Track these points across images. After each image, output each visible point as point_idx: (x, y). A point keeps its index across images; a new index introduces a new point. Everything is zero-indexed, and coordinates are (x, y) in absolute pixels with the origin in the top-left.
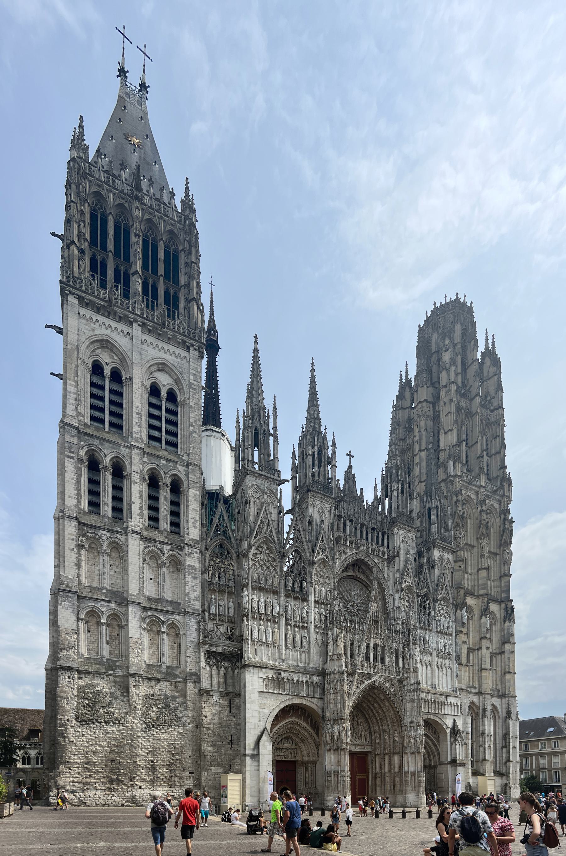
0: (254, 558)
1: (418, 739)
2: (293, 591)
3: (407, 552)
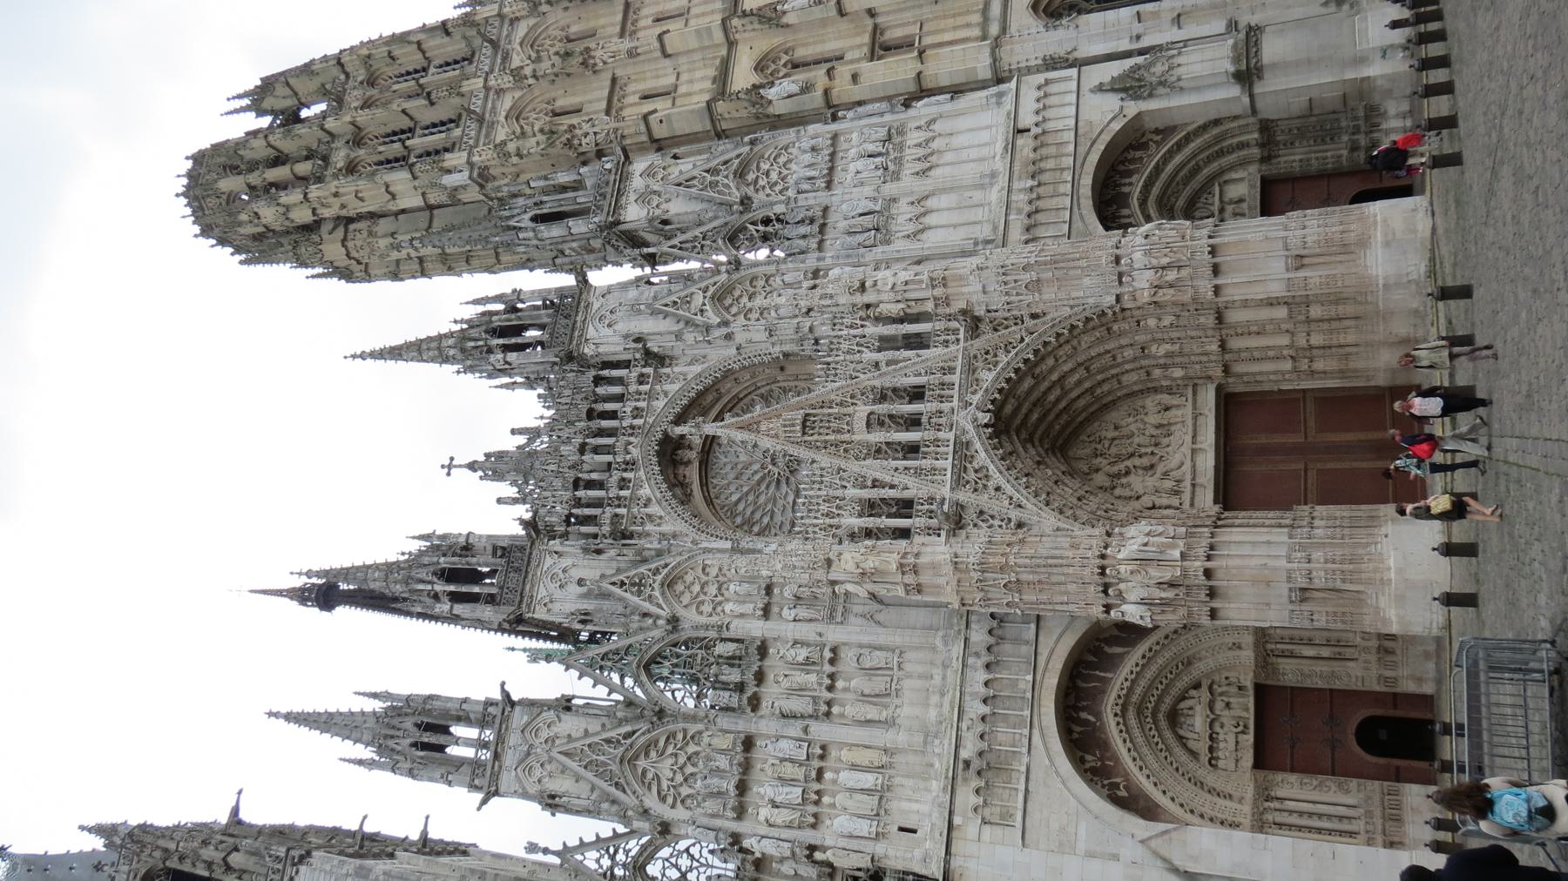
0: (670, 800)
1: (1165, 261)
2: (740, 688)
3: (635, 309)
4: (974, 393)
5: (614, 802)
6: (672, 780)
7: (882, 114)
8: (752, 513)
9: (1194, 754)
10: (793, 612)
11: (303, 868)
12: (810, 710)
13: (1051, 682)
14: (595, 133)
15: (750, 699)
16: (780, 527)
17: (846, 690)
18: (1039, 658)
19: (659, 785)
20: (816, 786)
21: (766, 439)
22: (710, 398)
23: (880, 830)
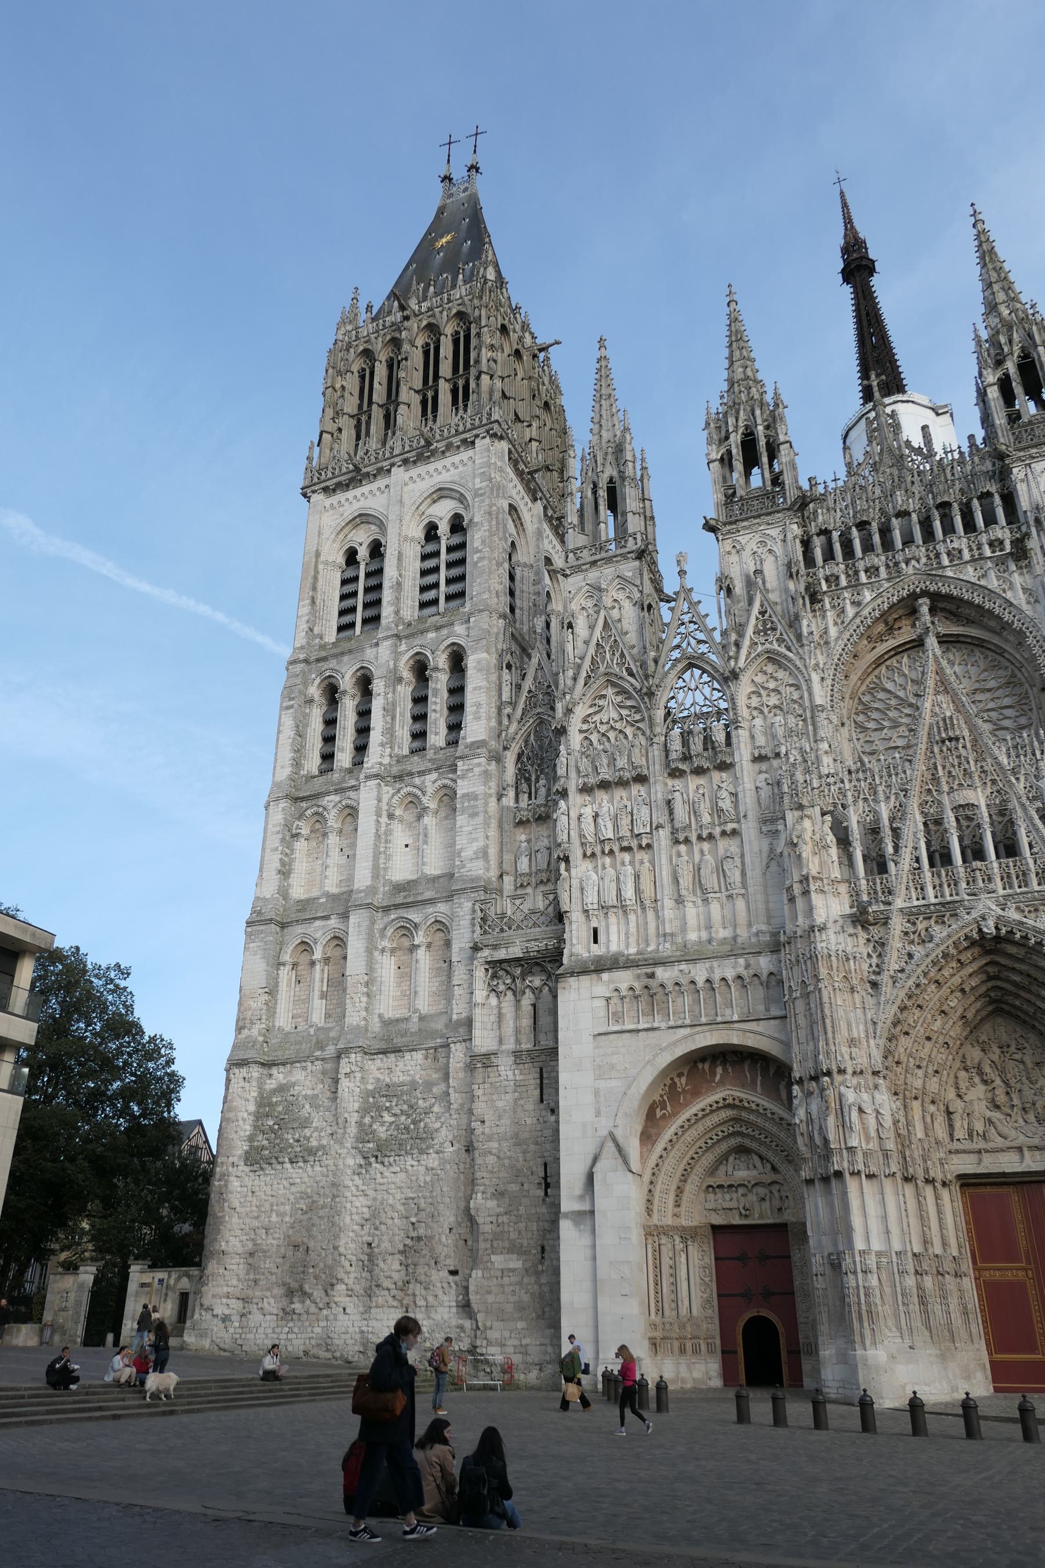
0: (585, 727)
4: (1018, 908)
5: (575, 679)
6: (601, 723)
8: (877, 709)
9: (712, 1171)
10: (763, 785)
11: (488, 440)
12: (678, 825)
13: (734, 1038)
15: (677, 769)
16: (867, 741)
17: (702, 852)
18: (754, 1023)
19: (595, 713)
20: (616, 849)
21: (928, 705)
22: (992, 623)
23: (591, 912)
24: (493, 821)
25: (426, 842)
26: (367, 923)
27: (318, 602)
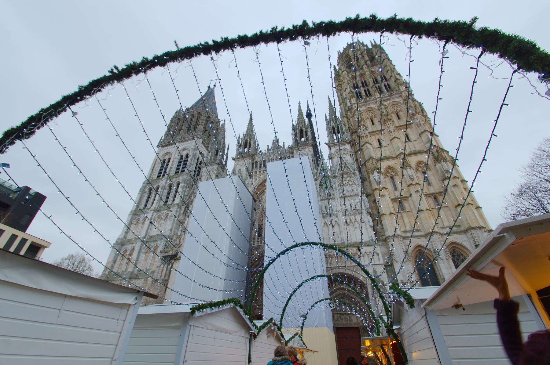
7: (365, 206)
14: (361, 132)
24: (175, 222)
25: (160, 227)
26: (140, 245)
27: (154, 170)
